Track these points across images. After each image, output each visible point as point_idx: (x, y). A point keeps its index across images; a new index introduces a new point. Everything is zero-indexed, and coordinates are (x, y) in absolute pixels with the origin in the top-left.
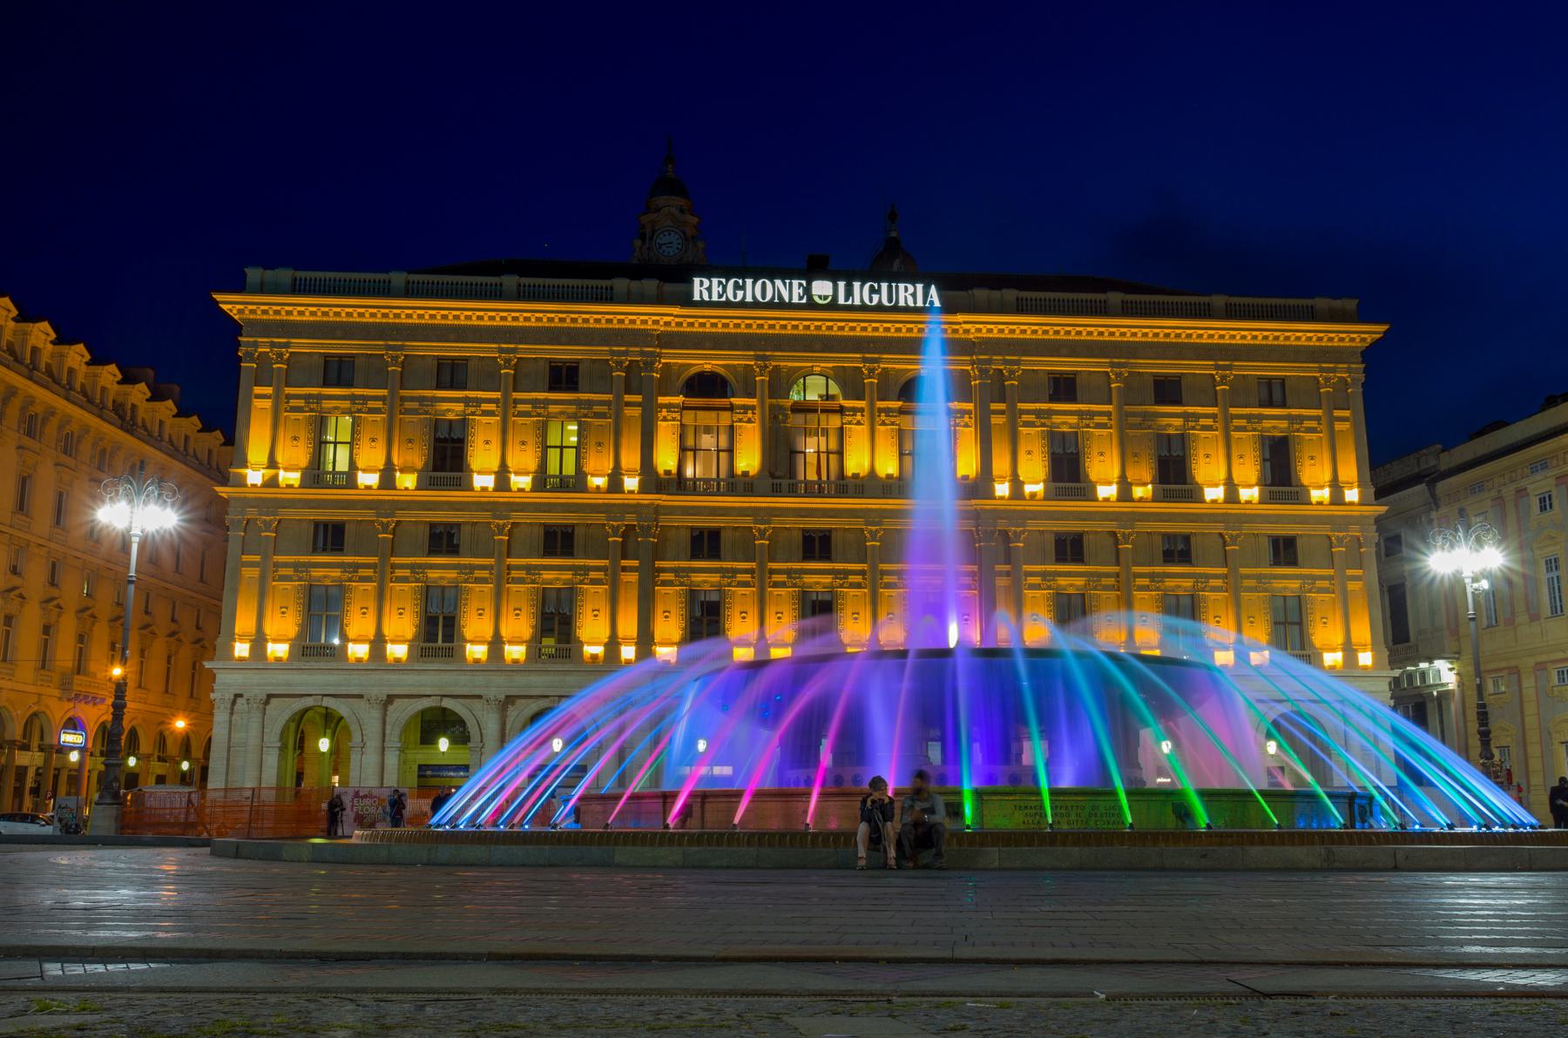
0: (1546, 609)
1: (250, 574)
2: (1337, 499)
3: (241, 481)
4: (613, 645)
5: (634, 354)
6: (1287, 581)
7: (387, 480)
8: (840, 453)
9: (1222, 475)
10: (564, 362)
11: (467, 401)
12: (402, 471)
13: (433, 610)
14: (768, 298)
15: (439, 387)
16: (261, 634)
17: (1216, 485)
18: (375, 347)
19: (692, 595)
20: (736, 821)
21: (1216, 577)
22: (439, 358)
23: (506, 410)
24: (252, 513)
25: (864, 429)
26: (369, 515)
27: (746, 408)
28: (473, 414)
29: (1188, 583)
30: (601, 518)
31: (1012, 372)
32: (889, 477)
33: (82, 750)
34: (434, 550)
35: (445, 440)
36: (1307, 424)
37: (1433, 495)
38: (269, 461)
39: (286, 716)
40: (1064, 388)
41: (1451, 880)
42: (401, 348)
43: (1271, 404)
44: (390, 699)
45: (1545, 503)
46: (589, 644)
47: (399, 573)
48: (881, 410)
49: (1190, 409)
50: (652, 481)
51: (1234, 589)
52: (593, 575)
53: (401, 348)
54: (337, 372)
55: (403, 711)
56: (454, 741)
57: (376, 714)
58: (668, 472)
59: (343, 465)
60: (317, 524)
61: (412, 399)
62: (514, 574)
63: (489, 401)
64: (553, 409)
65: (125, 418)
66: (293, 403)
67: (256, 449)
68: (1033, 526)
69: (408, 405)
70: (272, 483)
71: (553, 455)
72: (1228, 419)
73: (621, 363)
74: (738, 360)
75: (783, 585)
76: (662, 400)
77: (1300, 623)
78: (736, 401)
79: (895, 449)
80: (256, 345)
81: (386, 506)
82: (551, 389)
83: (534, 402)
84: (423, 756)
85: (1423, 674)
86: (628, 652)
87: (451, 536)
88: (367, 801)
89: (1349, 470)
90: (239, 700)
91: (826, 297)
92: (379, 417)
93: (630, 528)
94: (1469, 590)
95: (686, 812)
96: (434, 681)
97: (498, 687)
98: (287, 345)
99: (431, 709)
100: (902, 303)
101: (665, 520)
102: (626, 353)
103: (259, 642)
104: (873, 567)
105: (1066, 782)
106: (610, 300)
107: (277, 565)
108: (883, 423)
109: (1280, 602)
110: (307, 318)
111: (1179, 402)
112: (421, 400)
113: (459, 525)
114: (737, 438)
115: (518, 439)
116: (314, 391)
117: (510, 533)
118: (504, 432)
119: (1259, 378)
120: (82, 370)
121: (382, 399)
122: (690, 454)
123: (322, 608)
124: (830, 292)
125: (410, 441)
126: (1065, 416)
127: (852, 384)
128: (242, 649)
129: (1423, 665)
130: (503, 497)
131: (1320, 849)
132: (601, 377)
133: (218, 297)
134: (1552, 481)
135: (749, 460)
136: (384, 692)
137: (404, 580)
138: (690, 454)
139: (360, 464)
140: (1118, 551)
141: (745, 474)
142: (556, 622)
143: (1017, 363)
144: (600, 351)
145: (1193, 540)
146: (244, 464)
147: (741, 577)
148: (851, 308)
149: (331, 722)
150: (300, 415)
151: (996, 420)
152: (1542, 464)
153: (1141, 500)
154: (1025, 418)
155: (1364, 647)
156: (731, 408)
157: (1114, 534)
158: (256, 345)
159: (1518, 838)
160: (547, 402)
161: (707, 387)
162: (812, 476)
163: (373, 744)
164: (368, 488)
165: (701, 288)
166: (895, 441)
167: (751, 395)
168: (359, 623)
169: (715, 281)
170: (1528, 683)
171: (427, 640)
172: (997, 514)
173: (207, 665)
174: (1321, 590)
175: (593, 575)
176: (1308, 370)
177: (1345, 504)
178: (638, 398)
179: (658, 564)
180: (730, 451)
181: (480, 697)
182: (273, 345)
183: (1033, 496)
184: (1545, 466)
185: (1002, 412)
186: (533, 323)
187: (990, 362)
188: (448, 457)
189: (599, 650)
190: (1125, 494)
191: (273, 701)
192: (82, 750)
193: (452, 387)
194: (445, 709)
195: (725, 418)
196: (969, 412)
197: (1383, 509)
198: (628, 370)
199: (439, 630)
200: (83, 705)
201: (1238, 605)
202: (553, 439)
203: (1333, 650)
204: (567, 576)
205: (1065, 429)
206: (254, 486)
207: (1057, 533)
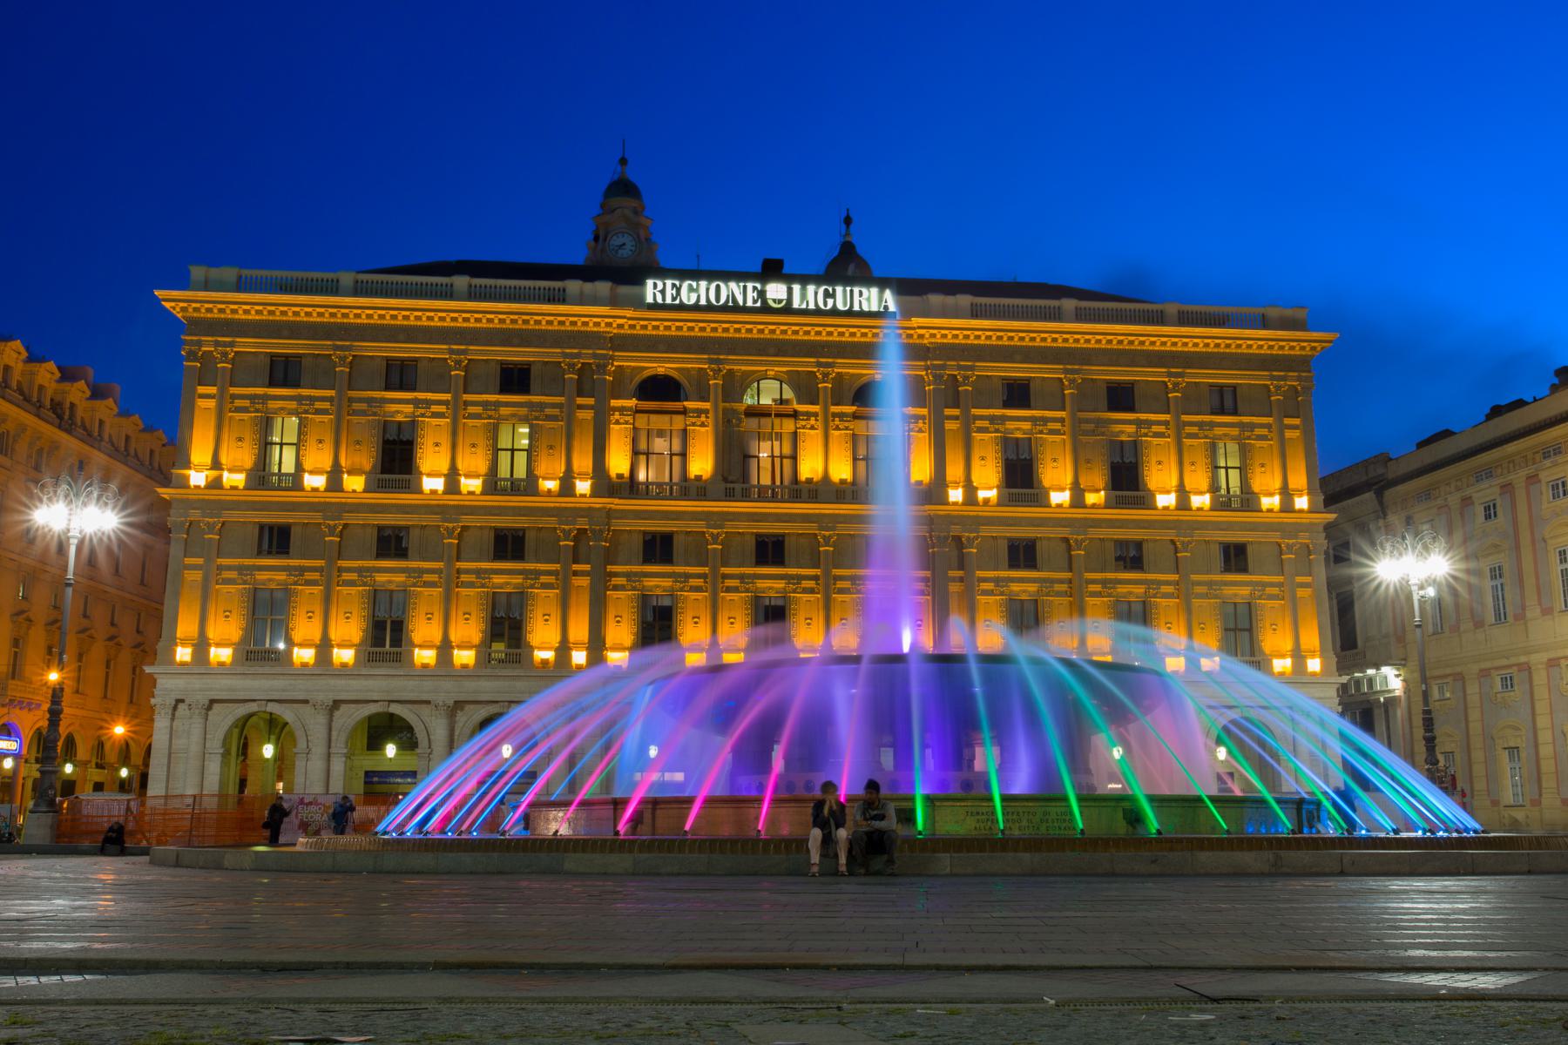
0: (1490, 617)
1: (196, 576)
2: (1287, 506)
3: (184, 483)
4: (564, 649)
5: (587, 356)
6: (1238, 587)
7: (335, 483)
8: (794, 458)
9: (1174, 482)
10: (515, 364)
11: (416, 403)
12: (350, 473)
13: (381, 614)
14: (722, 301)
15: (387, 388)
16: (205, 640)
17: (1168, 492)
18: (322, 347)
19: (644, 600)
20: (687, 828)
21: (1168, 583)
22: (388, 359)
23: (457, 412)
24: (195, 515)
25: (819, 433)
26: (317, 518)
27: (699, 412)
28: (423, 415)
29: (1140, 590)
30: (551, 522)
31: (966, 378)
32: (843, 482)
33: (17, 756)
34: (382, 554)
35: (394, 442)
36: (1258, 431)
37: (1381, 503)
38: (212, 464)
39: (230, 721)
40: (1018, 394)
41: (1397, 884)
42: (348, 348)
43: (1222, 412)
44: (337, 704)
45: (1490, 512)
46: (540, 649)
47: (346, 576)
48: (835, 415)
49: (1143, 416)
50: (605, 484)
51: (1185, 595)
52: (544, 579)
53: (348, 348)
54: (284, 372)
55: (351, 717)
56: (402, 747)
57: (322, 719)
58: (620, 476)
59: (289, 467)
60: (262, 527)
61: (360, 400)
62: (464, 578)
63: (439, 403)
64: (504, 411)
65: (61, 415)
66: (238, 403)
67: (200, 453)
68: (986, 531)
69: (356, 406)
70: (216, 484)
71: (504, 458)
72: (1180, 426)
73: (574, 365)
74: (692, 363)
75: (736, 590)
76: (614, 403)
77: (1250, 630)
78: (689, 405)
79: (849, 454)
81: (332, 507)
82: (502, 391)
83: (485, 404)
84: (369, 762)
85: (1371, 681)
86: (579, 657)
87: (399, 539)
88: (313, 808)
89: (1299, 479)
90: (181, 706)
91: (780, 301)
92: (326, 418)
93: (582, 532)
94: (1416, 598)
95: (636, 819)
96: (381, 687)
97: (447, 692)
98: (232, 344)
99: (378, 715)
100: (856, 308)
101: (619, 525)
102: (578, 356)
103: (201, 646)
104: (827, 573)
105: (1020, 787)
106: (563, 301)
107: (220, 568)
108: (837, 428)
109: (1230, 609)
110: (253, 316)
111: (1131, 409)
112: (370, 401)
113: (407, 528)
114: (691, 442)
115: (469, 441)
117: (460, 537)
118: (454, 434)
119: (1211, 385)
120: (18, 367)
121: (330, 399)
122: (643, 458)
123: (267, 612)
124: (784, 296)
125: (358, 443)
126: (1019, 422)
127: (806, 388)
128: (183, 654)
129: (1370, 672)
130: (453, 500)
131: (1268, 855)
132: (554, 382)
134: (1497, 490)
135: (702, 464)
136: (329, 698)
137: (352, 583)
138: (643, 458)
139: (307, 465)
140: (1070, 557)
141: (698, 478)
142: (506, 627)
143: (971, 368)
144: (552, 354)
145: (1145, 546)
146: (187, 464)
147: (694, 582)
148: (805, 312)
149: (275, 727)
150: (245, 416)
151: (950, 426)
152: (1487, 473)
153: (1094, 506)
154: (979, 423)
155: (1313, 654)
156: (684, 412)
157: (1066, 540)
158: (199, 344)
159: (1462, 843)
160: (498, 404)
161: (660, 390)
162: (766, 480)
163: (319, 750)
164: (315, 490)
165: (652, 290)
166: (849, 445)
167: (704, 399)
168: (305, 627)
169: (669, 283)
170: (1473, 689)
171: (374, 645)
172: (951, 520)
173: (148, 670)
174: (1271, 597)
175: (544, 579)
176: (1259, 378)
177: (1294, 511)
178: (591, 401)
179: (610, 568)
180: (684, 455)
181: (428, 702)
182: (217, 344)
183: (986, 501)
184: (1490, 475)
185: (957, 418)
186: (484, 324)
187: (943, 367)
188: (397, 458)
190: (1078, 501)
191: (216, 706)
192: (17, 756)
193: (401, 388)
194: (392, 715)
195: (679, 422)
196: (923, 418)
197: (1332, 517)
198: (581, 372)
199: (387, 634)
200: (17, 711)
201: (1189, 611)
202: (504, 442)
203: (1282, 656)
204: (518, 580)
205: (1019, 435)
207: (1010, 540)
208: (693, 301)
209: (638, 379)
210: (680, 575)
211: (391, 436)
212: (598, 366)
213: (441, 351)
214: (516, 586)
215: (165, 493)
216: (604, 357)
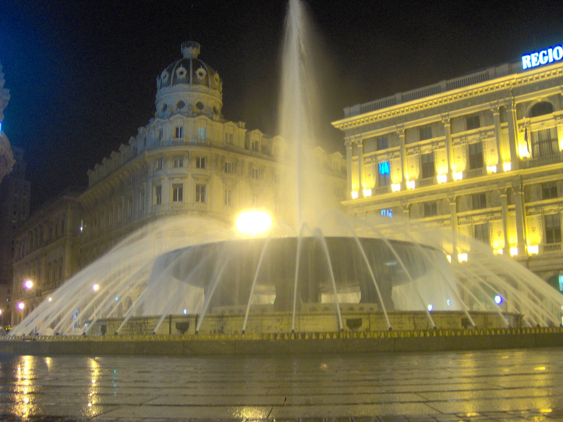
5: (501, 102)
11: (432, 143)
28: (436, 148)
30: (495, 187)
50: (518, 164)
93: (509, 189)
101: (526, 183)
116: (373, 153)
133: (334, 123)
158: (350, 139)
160: (466, 136)
165: (527, 61)
169: (533, 55)
182: (356, 138)
189: (501, 252)
206: (355, 199)
208: (545, 62)
209: (529, 107)
211: (426, 161)
212: (507, 106)
213: (437, 118)
214: (484, 220)
215: (343, 203)
216: (510, 100)
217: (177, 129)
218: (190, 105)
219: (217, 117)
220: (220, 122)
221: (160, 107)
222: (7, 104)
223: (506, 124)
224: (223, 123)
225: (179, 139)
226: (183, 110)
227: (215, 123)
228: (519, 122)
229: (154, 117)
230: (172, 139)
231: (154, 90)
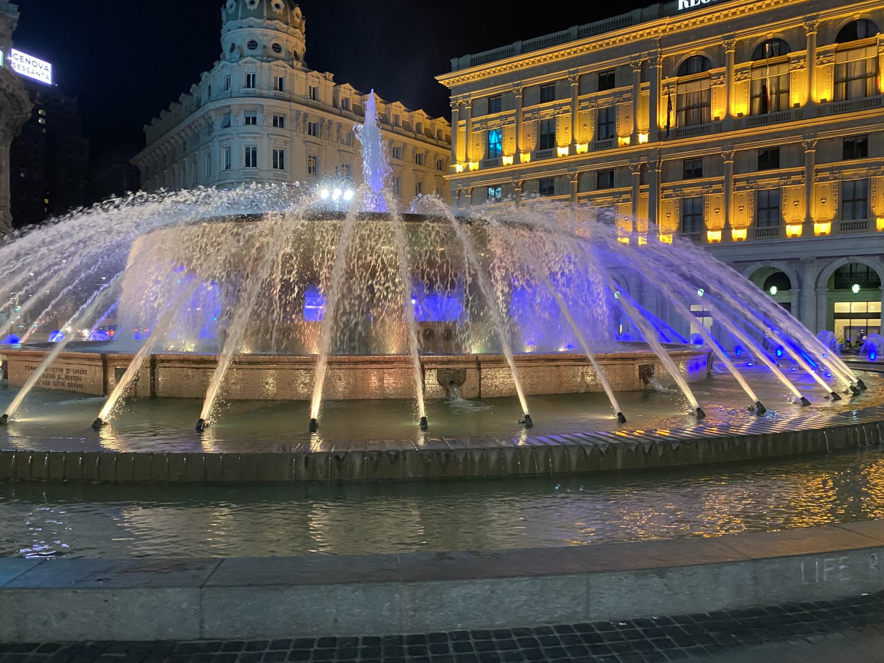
3: (453, 171)
27: (719, 75)
30: (626, 162)
53: (520, 84)
54: (494, 105)
70: (467, 170)
74: (713, 42)
75: (744, 188)
80: (456, 99)
83: (590, 100)
98: (470, 96)
102: (639, 57)
132: (628, 78)
133: (437, 78)
141: (717, 119)
158: (456, 99)
186: (585, 52)
210: (706, 183)
212: (652, 60)
216: (656, 53)
217: (249, 76)
218: (265, 47)
219: (298, 64)
220: (302, 70)
221: (226, 47)
222: (15, 25)
223: (648, 84)
224: (307, 72)
225: (251, 89)
226: (254, 52)
227: (295, 71)
228: (663, 82)
229: (219, 59)
230: (243, 90)
231: (219, 24)
